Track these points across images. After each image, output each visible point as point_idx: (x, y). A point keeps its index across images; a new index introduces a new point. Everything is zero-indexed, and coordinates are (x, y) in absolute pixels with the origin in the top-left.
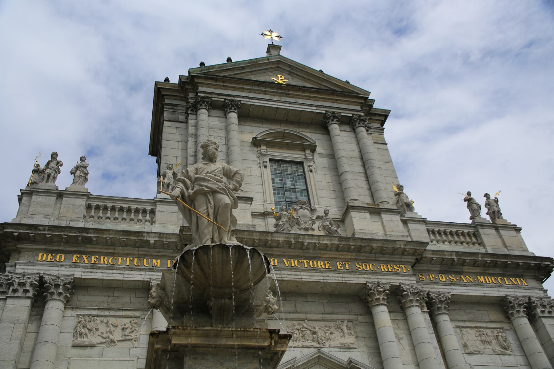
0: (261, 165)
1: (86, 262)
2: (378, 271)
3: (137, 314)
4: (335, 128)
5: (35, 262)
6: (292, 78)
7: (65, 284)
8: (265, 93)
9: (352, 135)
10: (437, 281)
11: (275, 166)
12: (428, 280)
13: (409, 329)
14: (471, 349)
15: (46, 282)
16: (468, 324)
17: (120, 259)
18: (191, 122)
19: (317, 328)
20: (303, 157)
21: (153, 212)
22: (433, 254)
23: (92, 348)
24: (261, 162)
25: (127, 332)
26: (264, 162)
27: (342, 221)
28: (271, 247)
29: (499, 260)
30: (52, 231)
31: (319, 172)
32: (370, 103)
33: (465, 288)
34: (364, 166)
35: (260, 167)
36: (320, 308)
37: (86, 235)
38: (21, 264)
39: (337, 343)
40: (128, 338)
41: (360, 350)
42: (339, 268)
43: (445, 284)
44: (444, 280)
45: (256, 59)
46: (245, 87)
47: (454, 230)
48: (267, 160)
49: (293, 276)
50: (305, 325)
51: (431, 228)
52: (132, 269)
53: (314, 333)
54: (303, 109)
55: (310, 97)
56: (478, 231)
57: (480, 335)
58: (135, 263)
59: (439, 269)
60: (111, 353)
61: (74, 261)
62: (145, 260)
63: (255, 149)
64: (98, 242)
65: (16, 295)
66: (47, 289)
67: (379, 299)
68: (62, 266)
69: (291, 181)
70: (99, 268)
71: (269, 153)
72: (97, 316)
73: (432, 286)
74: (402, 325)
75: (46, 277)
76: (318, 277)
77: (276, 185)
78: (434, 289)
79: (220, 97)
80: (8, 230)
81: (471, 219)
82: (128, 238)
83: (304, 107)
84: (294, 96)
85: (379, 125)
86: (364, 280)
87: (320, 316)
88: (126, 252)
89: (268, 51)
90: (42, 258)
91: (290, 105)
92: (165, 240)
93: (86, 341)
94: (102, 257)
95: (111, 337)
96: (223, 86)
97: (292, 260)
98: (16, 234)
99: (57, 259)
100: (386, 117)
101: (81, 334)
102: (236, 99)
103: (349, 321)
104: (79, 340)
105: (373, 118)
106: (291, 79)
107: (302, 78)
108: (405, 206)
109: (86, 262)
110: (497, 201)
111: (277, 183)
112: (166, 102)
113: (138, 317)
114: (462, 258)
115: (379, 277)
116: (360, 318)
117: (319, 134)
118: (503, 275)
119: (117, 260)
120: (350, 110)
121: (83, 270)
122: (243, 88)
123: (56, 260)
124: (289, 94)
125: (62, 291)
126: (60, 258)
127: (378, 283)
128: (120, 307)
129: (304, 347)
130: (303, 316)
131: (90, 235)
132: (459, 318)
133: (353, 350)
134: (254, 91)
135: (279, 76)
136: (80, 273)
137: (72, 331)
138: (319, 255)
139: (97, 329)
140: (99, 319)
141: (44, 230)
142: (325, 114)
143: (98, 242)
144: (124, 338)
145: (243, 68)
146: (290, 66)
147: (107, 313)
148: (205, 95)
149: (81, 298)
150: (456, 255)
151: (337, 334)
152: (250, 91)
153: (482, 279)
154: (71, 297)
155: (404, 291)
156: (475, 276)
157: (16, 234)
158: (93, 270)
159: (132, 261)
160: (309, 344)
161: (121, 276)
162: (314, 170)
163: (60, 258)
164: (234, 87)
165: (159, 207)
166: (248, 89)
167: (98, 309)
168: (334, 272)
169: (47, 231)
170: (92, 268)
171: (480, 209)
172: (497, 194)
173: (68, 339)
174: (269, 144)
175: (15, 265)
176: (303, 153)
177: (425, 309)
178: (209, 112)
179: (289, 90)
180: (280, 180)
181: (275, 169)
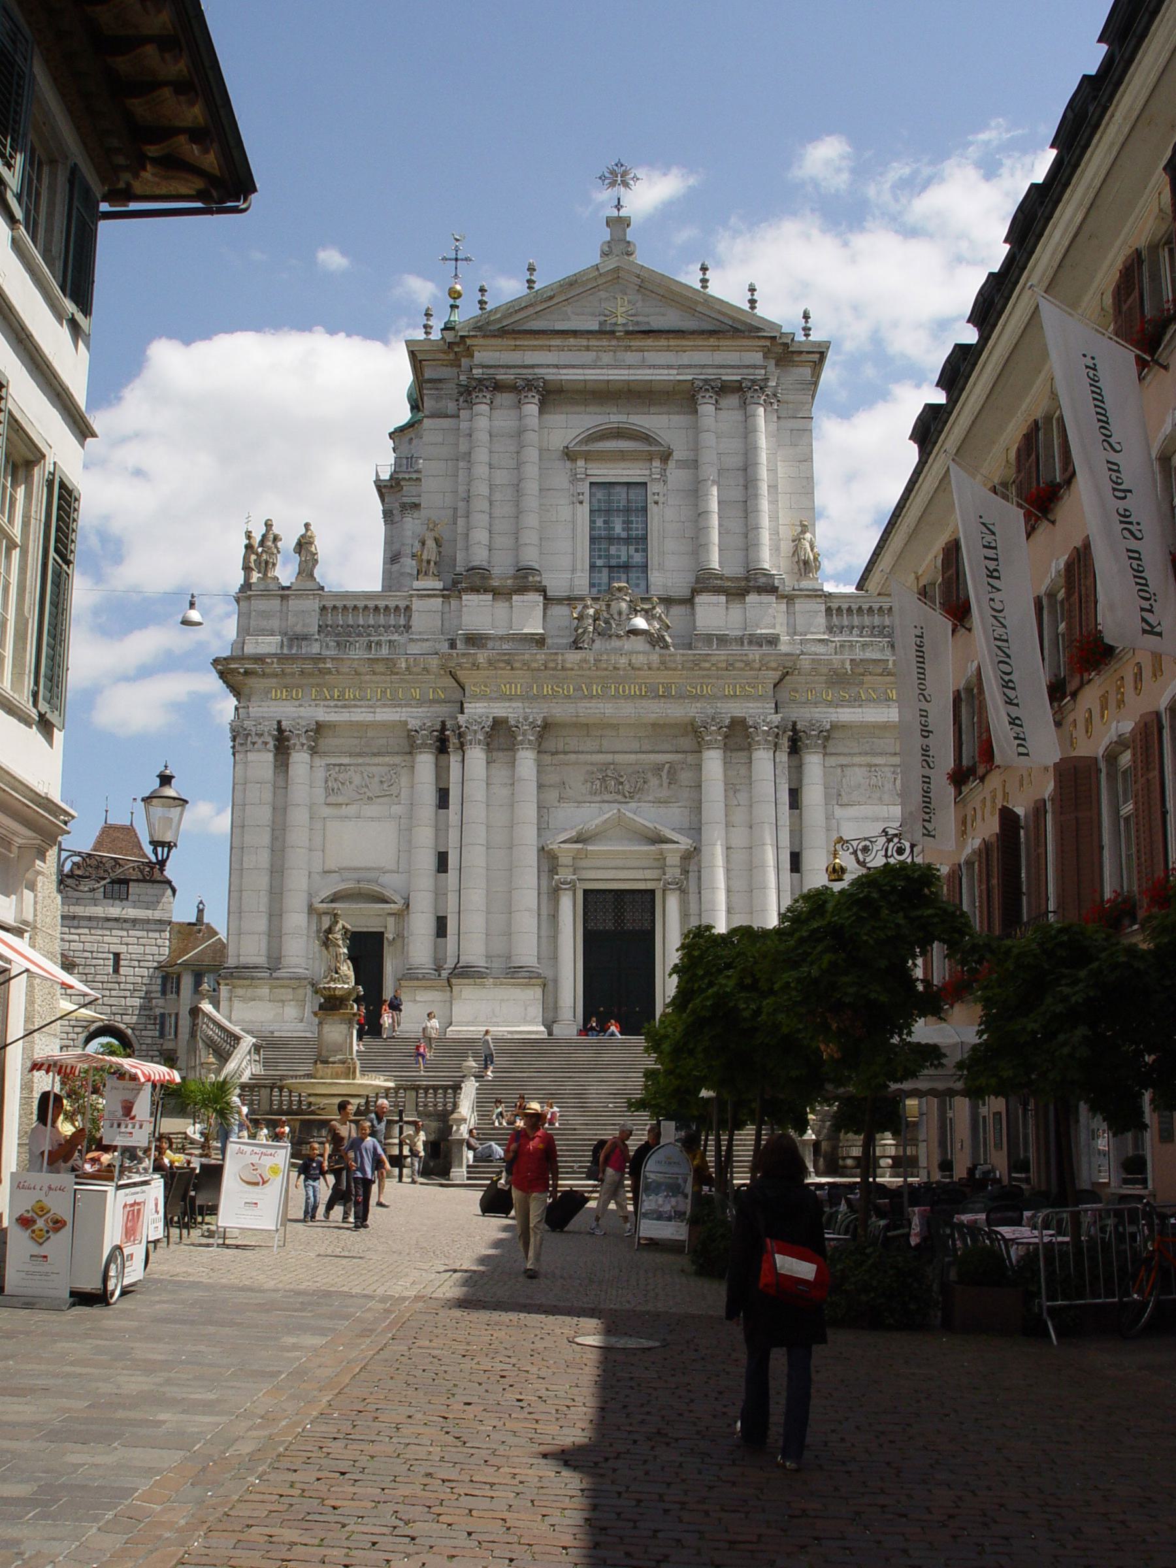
0: (575, 500)
2: (719, 694)
4: (707, 409)
6: (643, 300)
7: (307, 731)
9: (737, 416)
11: (600, 494)
12: (803, 699)
13: (751, 777)
14: (845, 800)
15: (285, 731)
16: (857, 760)
18: (464, 425)
20: (647, 472)
21: (408, 608)
25: (385, 785)
26: (579, 494)
32: (785, 340)
34: (746, 487)
35: (573, 503)
39: (651, 798)
41: (679, 804)
42: (661, 693)
43: (830, 704)
45: (575, 275)
48: (585, 488)
52: (385, 706)
54: (654, 378)
57: (870, 777)
60: (370, 810)
61: (313, 697)
63: (568, 464)
69: (624, 522)
71: (589, 472)
75: (283, 723)
77: (596, 533)
80: (232, 666)
85: (806, 372)
90: (276, 696)
91: (632, 371)
93: (340, 800)
100: (822, 355)
102: (537, 371)
104: (332, 799)
105: (796, 359)
106: (639, 304)
107: (660, 297)
108: (802, 565)
112: (427, 376)
116: (690, 758)
123: (292, 698)
125: (305, 742)
126: (297, 695)
129: (603, 802)
132: (846, 750)
133: (671, 805)
142: (692, 382)
145: (551, 298)
151: (654, 781)
152: (561, 349)
154: (317, 745)
155: (751, 727)
157: (242, 670)
158: (337, 710)
161: (372, 715)
162: (661, 499)
163: (297, 695)
165: (416, 604)
170: (336, 706)
173: (320, 793)
174: (588, 456)
176: (647, 465)
180: (605, 522)
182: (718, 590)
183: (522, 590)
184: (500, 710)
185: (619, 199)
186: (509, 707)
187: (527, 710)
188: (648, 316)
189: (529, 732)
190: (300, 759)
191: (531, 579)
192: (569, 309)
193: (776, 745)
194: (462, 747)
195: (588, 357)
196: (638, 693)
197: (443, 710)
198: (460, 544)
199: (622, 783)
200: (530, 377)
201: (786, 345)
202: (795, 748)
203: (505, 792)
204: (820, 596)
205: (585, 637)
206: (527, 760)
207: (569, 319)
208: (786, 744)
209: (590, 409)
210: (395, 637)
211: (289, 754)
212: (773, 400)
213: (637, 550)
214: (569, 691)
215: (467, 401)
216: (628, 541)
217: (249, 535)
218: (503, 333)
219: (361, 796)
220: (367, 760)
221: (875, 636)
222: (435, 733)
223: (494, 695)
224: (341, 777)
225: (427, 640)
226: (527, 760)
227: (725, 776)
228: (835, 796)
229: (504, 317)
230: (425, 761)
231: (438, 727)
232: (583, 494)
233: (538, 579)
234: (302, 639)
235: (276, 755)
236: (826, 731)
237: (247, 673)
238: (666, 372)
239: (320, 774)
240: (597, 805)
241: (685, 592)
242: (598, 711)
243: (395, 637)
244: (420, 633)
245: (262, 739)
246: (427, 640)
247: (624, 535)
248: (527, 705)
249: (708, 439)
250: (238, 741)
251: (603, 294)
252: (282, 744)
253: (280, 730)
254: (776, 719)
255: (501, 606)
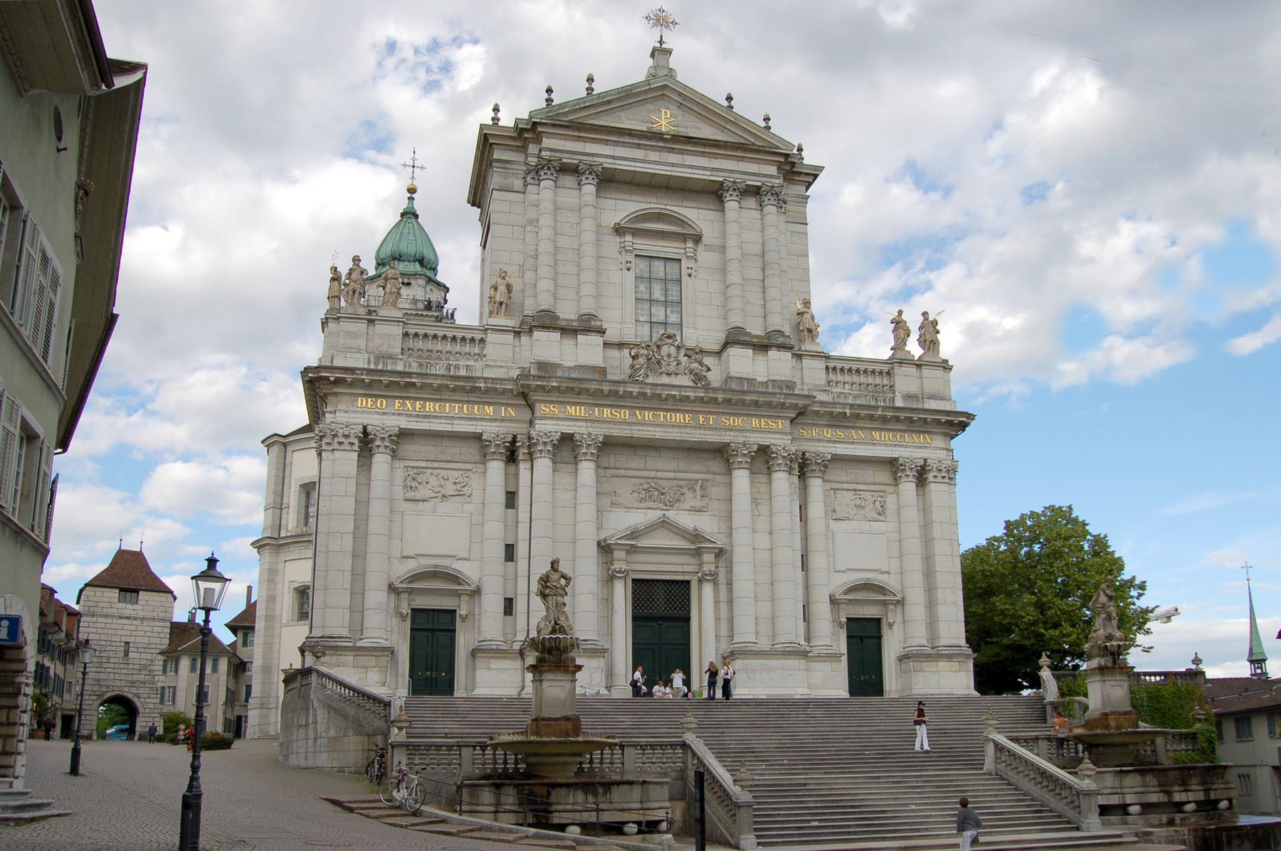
0: (624, 266)
1: (411, 409)
2: (748, 427)
3: (468, 466)
4: (731, 205)
5: (355, 409)
6: (682, 115)
7: (390, 436)
8: (638, 146)
10: (821, 437)
11: (643, 265)
17: (448, 405)
19: (666, 489)
20: (682, 251)
21: (482, 341)
22: (821, 407)
23: (425, 503)
24: (624, 262)
26: (627, 262)
27: (719, 353)
28: (622, 397)
29: (902, 415)
30: (371, 375)
31: (700, 276)
33: (852, 446)
36: (674, 465)
37: (408, 380)
38: (341, 411)
39: (687, 506)
40: (461, 493)
43: (829, 441)
44: (829, 436)
46: (610, 138)
47: (862, 367)
49: (644, 433)
50: (653, 485)
51: (831, 365)
53: (663, 494)
54: (691, 176)
55: (704, 152)
56: (893, 368)
58: (465, 411)
59: (826, 423)
62: (476, 406)
63: (618, 239)
64: (424, 387)
65: (342, 447)
66: (373, 441)
67: (741, 462)
68: (384, 414)
69: (661, 289)
70: (425, 417)
71: (635, 246)
72: (426, 468)
73: (812, 444)
74: (764, 489)
76: (675, 435)
77: (639, 296)
78: (810, 448)
79: (572, 156)
80: (323, 374)
81: (892, 349)
82: (456, 384)
83: (693, 171)
84: (682, 152)
86: (729, 438)
87: (672, 475)
88: (454, 398)
89: (652, 55)
90: (362, 404)
91: (674, 169)
92: (498, 386)
93: (418, 495)
94: (428, 403)
95: (442, 491)
96: (579, 137)
97: (647, 413)
98: (332, 379)
99: (379, 406)
101: (411, 488)
102: (596, 159)
103: (704, 480)
104: (410, 494)
106: (680, 118)
108: (806, 333)
109: (411, 409)
110: (937, 323)
111: (642, 292)
113: (471, 470)
114: (857, 412)
115: (748, 435)
116: (718, 478)
117: (711, 210)
118: (905, 431)
119: (445, 406)
120: (759, 175)
121: (407, 419)
122: (607, 140)
123: (377, 407)
124: (673, 148)
126: (381, 404)
127: (744, 444)
128: (450, 458)
129: (649, 508)
130: (653, 474)
131: (413, 380)
134: (624, 144)
135: (663, 111)
136: (405, 423)
137: (402, 484)
138: (679, 408)
139: (427, 483)
140: (428, 471)
141: (362, 374)
142: (722, 183)
143: (424, 387)
144: (457, 493)
145: (609, 102)
146: (681, 94)
147: (436, 465)
148: (552, 153)
149: (407, 447)
150: (850, 409)
151: (689, 494)
152: (616, 144)
153: (876, 435)
155: (773, 453)
156: (869, 432)
158: (418, 419)
159: (461, 409)
160: (655, 507)
161: (451, 426)
162: (693, 275)
163: (381, 404)
164: (594, 139)
165: (491, 337)
166: (614, 141)
167: (427, 461)
168: (695, 427)
169: (366, 375)
170: (418, 416)
171: (908, 336)
172: (939, 313)
173: (399, 492)
174: (637, 233)
175: (335, 412)
176: (683, 246)
177: (796, 472)
178: (555, 182)
179: (674, 143)
181: (641, 270)
182: (746, 344)
183: (587, 330)
184: (567, 428)
185: (661, 36)
186: (575, 426)
187: (590, 429)
188: (687, 128)
189: (593, 447)
190: (381, 461)
191: (593, 323)
192: (622, 114)
193: (790, 468)
194: (531, 458)
195: (639, 154)
196: (682, 421)
197: (514, 428)
198: (528, 292)
199: (663, 494)
200: (593, 163)
201: (793, 164)
202: (802, 476)
203: (569, 495)
204: (822, 357)
205: (641, 372)
206: (587, 470)
207: (622, 123)
208: (797, 469)
209: (634, 198)
210: (471, 363)
211: (371, 456)
212: (781, 203)
213: (672, 312)
214: (625, 416)
215: (534, 178)
216: (666, 303)
217: (334, 269)
218: (571, 126)
219: (436, 495)
220: (442, 465)
221: (862, 391)
222: (507, 444)
223: (561, 416)
224: (420, 478)
225: (501, 367)
226: (587, 470)
227: (752, 493)
228: (833, 514)
229: (571, 112)
230: (496, 468)
231: (510, 439)
232: (630, 262)
233: (600, 324)
234: (388, 358)
235: (359, 456)
236: (828, 461)
237: (338, 382)
238: (701, 172)
239: (400, 474)
240: (643, 511)
241: (716, 348)
242: (649, 433)
243: (471, 363)
244: (494, 361)
245: (349, 440)
246: (501, 367)
247: (662, 299)
248: (589, 424)
249: (732, 228)
250: (325, 440)
251: (650, 107)
252: (366, 443)
253: (365, 432)
254: (793, 449)
255: (568, 343)
